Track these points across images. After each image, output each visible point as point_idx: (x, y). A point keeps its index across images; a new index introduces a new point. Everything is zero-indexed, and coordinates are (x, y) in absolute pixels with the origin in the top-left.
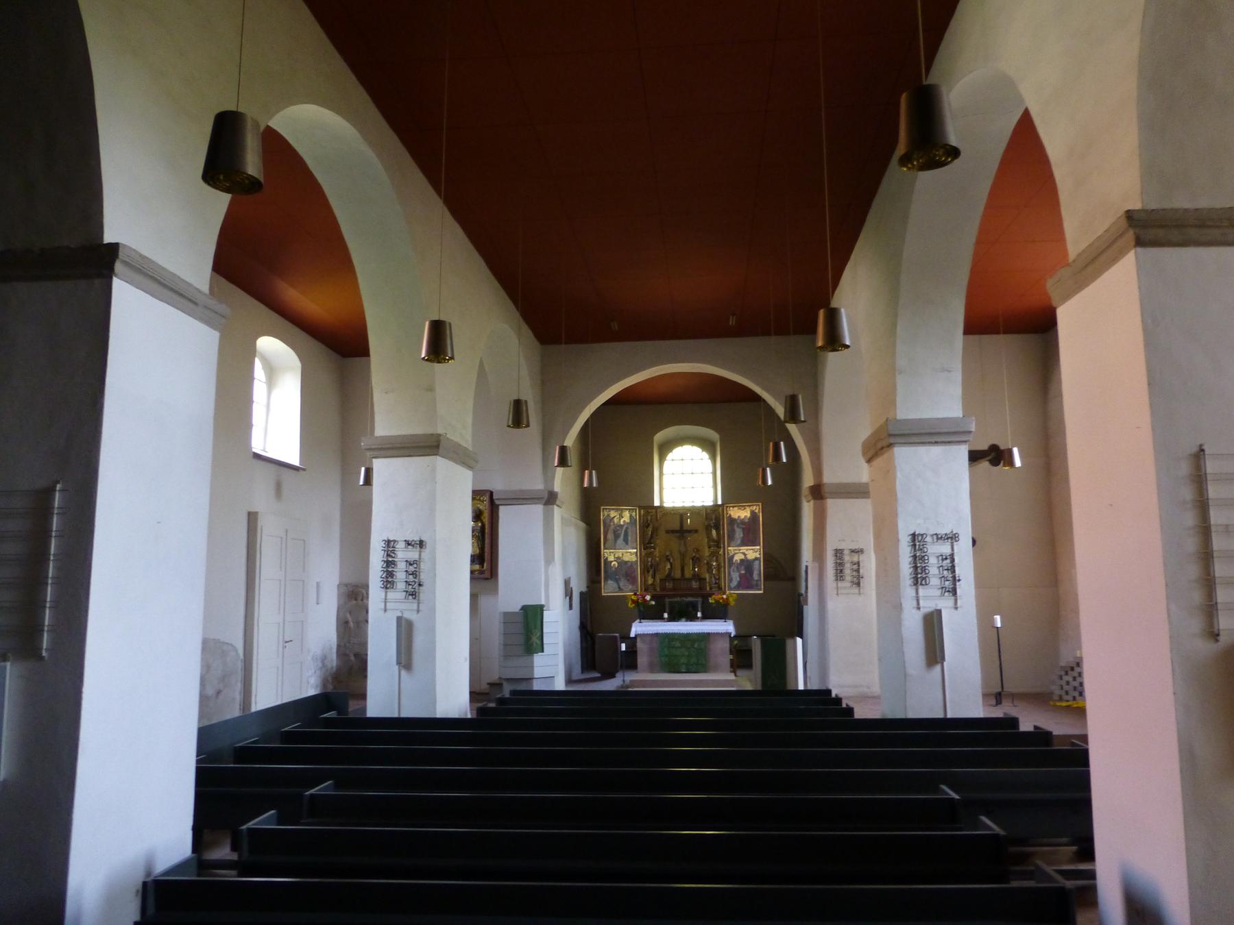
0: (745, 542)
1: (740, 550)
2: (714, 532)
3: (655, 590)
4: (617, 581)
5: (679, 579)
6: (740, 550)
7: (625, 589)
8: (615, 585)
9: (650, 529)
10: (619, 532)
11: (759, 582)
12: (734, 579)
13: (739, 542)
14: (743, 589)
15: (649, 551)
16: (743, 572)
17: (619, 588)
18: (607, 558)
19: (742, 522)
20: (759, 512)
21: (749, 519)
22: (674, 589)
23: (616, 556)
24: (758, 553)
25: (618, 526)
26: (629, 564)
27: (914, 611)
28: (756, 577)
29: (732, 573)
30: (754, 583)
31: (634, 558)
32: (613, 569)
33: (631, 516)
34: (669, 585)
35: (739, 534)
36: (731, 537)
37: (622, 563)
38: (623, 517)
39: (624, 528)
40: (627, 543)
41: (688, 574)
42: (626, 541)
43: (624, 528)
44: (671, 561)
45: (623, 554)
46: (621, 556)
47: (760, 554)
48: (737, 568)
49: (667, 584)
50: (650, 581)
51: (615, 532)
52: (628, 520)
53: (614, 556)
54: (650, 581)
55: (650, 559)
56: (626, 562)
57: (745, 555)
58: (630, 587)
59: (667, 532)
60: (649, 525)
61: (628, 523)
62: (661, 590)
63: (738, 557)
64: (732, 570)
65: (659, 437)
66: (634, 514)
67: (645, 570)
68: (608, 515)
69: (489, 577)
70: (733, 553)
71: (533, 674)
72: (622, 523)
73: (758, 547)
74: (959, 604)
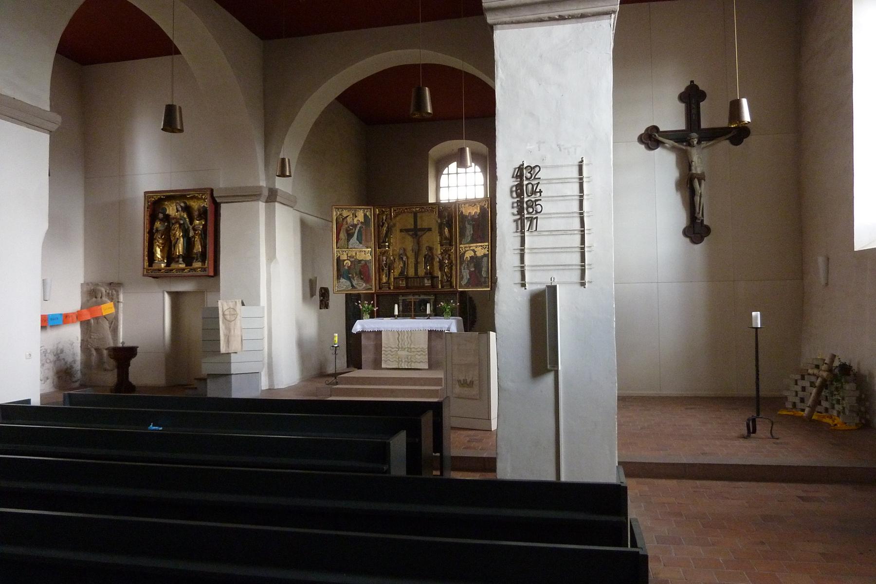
0: (474, 241)
1: (470, 247)
2: (446, 230)
3: (390, 288)
4: (349, 279)
5: (413, 278)
6: (470, 247)
8: (348, 283)
10: (351, 231)
11: (487, 280)
12: (465, 277)
13: (469, 238)
14: (473, 287)
15: (383, 250)
16: (473, 269)
17: (352, 286)
18: (340, 257)
19: (473, 218)
20: (488, 208)
21: (478, 215)
22: (407, 287)
23: (349, 255)
24: (486, 249)
25: (352, 226)
27: (518, 289)
28: (484, 274)
29: (463, 271)
30: (483, 280)
31: (369, 257)
32: (346, 268)
33: (365, 216)
34: (403, 284)
35: (469, 231)
36: (462, 234)
37: (356, 262)
38: (356, 217)
40: (360, 243)
41: (421, 272)
42: (360, 240)
44: (404, 259)
45: (356, 254)
47: (488, 251)
48: (468, 264)
51: (347, 231)
53: (347, 255)
55: (384, 258)
57: (475, 252)
58: (364, 284)
59: (401, 231)
60: (383, 224)
61: (362, 223)
62: (394, 288)
63: (469, 255)
64: (463, 268)
65: (435, 152)
67: (380, 270)
68: (341, 215)
69: (212, 274)
70: (464, 250)
71: (230, 370)
72: (355, 222)
73: (487, 244)
74: (587, 278)
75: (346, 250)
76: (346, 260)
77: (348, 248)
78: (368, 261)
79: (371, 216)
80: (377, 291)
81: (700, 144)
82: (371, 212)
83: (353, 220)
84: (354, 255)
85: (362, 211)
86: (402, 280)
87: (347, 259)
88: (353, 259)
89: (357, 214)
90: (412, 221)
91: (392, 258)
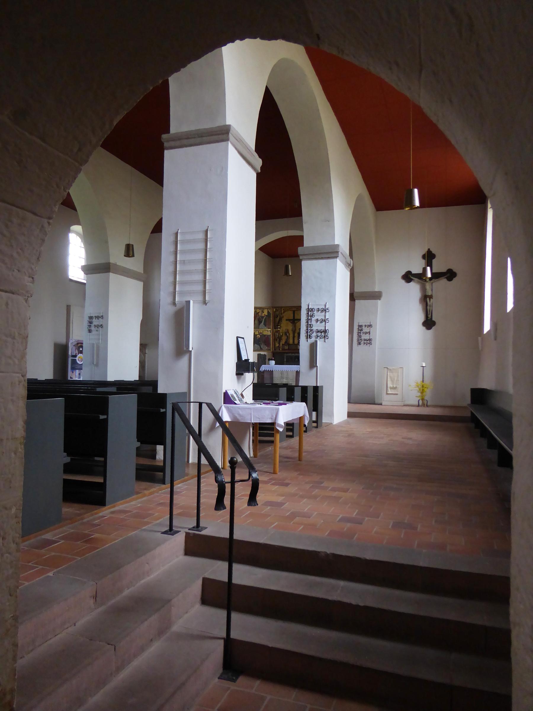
3: (280, 350)
5: (292, 344)
7: (264, 349)
8: (259, 346)
9: (279, 317)
15: (277, 330)
17: (261, 348)
22: (289, 349)
25: (261, 317)
26: (266, 336)
31: (269, 333)
32: (258, 338)
33: (268, 312)
34: (286, 347)
38: (263, 312)
39: (264, 318)
40: (265, 326)
43: (264, 318)
44: (287, 335)
46: (262, 332)
49: (285, 347)
50: (277, 345)
52: (267, 314)
54: (277, 345)
55: (278, 334)
56: (265, 335)
58: (267, 347)
59: (287, 320)
60: (277, 316)
66: (270, 311)
67: (275, 340)
72: (263, 315)
75: (258, 329)
76: (257, 335)
77: (259, 329)
78: (269, 335)
79: (271, 312)
80: (273, 351)
81: (430, 281)
82: (271, 310)
83: (262, 314)
84: (262, 332)
85: (266, 310)
86: (286, 346)
87: (258, 334)
88: (261, 335)
89: (264, 311)
90: (292, 315)
91: (281, 334)
